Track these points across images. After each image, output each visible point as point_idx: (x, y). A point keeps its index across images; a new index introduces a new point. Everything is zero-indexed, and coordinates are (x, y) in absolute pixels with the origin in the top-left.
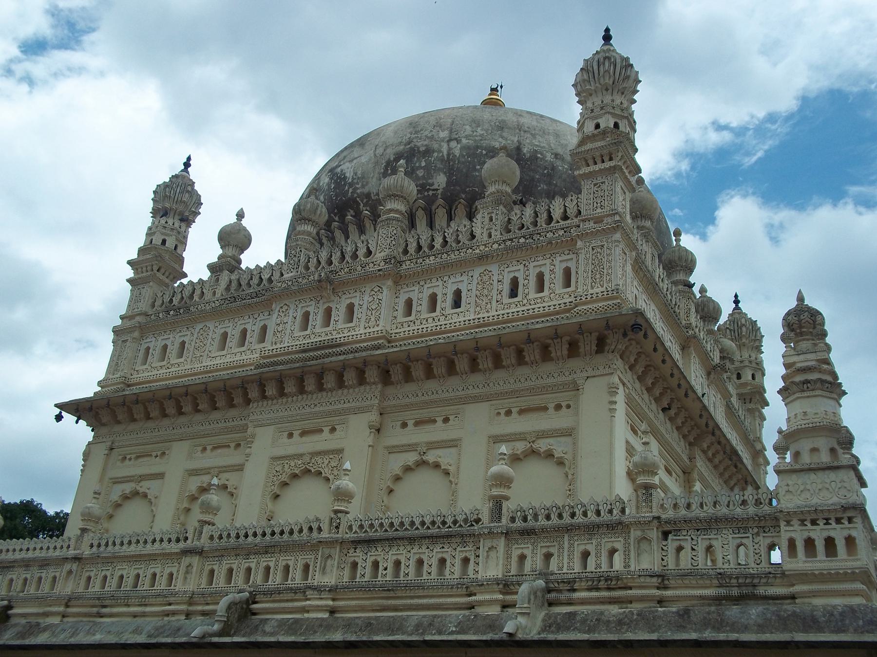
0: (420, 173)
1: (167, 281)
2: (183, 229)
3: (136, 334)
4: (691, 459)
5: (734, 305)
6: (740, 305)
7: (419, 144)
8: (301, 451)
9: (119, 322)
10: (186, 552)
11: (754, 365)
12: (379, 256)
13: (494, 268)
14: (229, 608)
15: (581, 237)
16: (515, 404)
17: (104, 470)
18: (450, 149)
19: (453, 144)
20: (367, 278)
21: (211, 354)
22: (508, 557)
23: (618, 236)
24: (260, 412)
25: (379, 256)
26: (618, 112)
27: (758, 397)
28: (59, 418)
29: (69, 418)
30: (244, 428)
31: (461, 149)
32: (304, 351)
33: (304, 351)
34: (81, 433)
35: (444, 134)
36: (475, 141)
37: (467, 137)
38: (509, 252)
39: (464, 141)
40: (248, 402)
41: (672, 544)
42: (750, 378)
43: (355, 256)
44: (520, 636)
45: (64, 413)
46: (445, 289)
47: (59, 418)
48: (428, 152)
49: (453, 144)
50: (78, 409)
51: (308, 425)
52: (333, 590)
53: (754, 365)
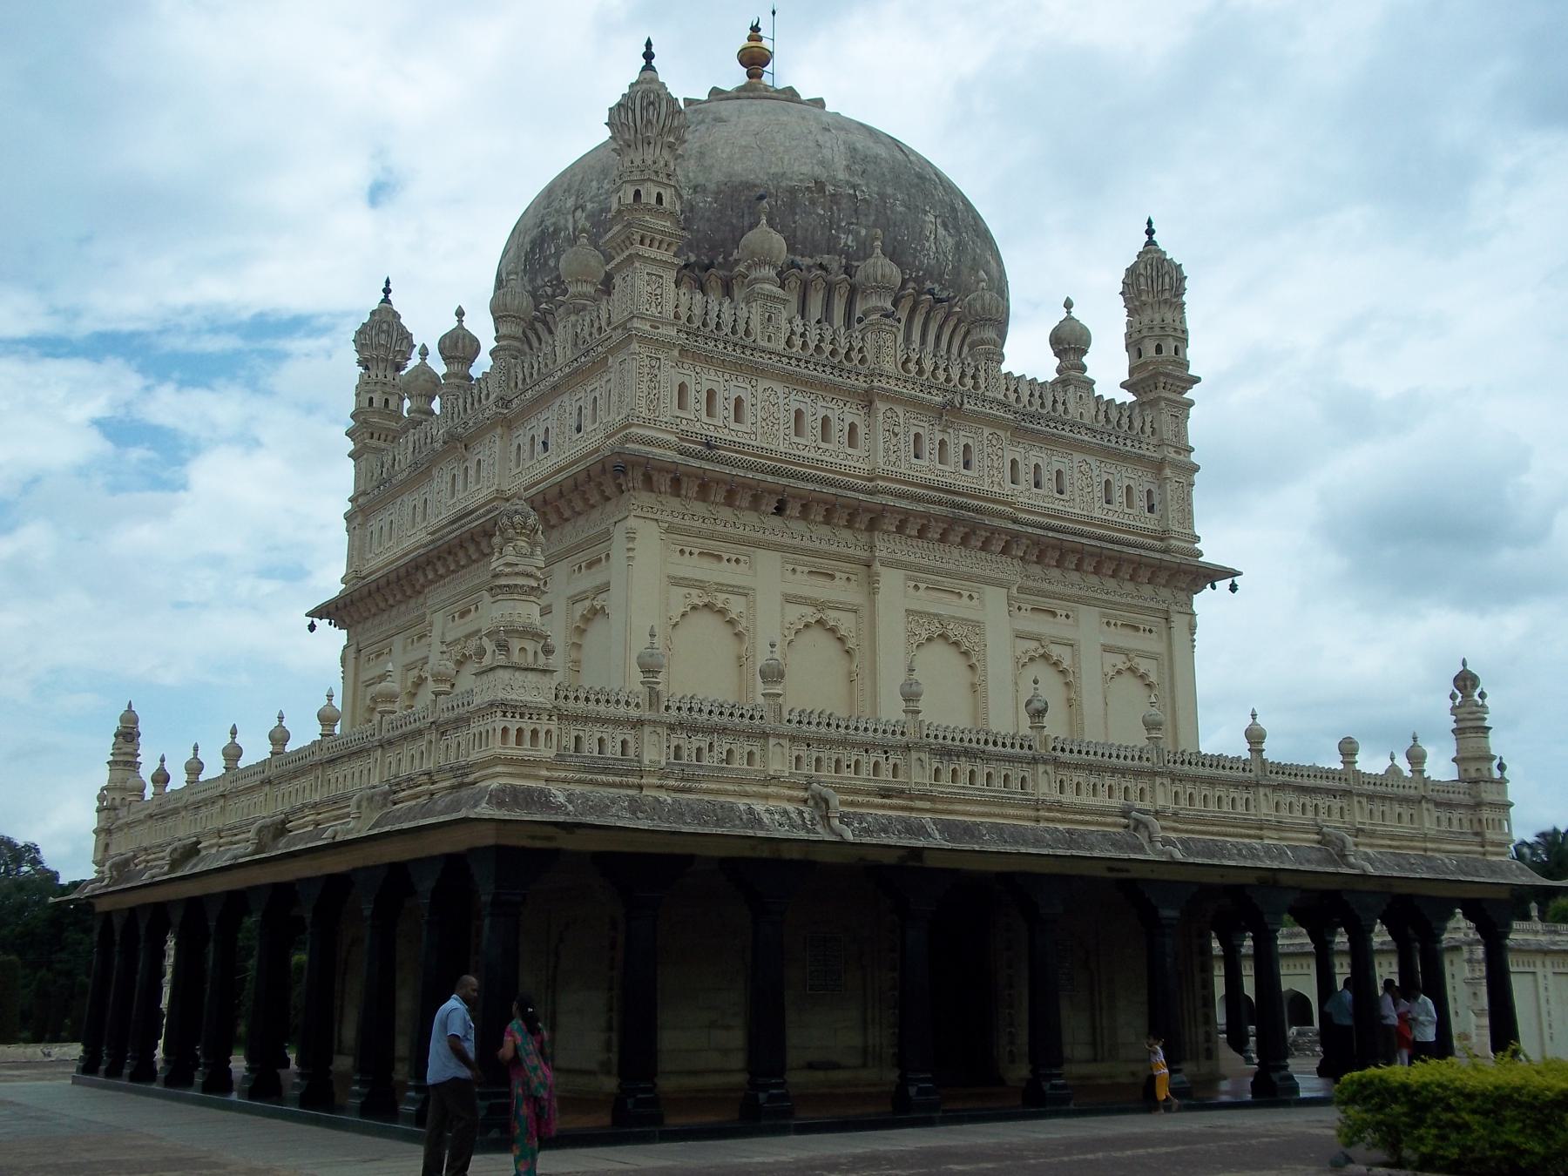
0: (552, 263)
1: (382, 445)
2: (390, 377)
3: (359, 520)
4: (872, 548)
5: (1146, 238)
6: (1155, 237)
7: (548, 223)
8: (460, 635)
9: (349, 506)
10: (262, 783)
11: (1157, 331)
12: (492, 397)
13: (566, 397)
14: (260, 831)
15: (611, 351)
16: (584, 557)
17: (356, 675)
18: (575, 222)
19: (579, 213)
20: (483, 430)
21: (409, 533)
22: (382, 766)
23: (635, 346)
24: (437, 596)
25: (492, 397)
26: (636, 176)
27: (1162, 379)
28: (312, 627)
29: (322, 624)
30: (422, 618)
31: (587, 218)
32: (453, 522)
33: (453, 522)
34: (333, 638)
35: (570, 203)
36: (600, 202)
37: (591, 201)
38: (578, 375)
39: (589, 206)
40: (423, 587)
41: (443, 744)
42: (1152, 352)
43: (480, 401)
44: (338, 839)
45: (316, 621)
46: (535, 427)
47: (312, 627)
48: (556, 231)
49: (579, 213)
50: (330, 611)
51: (460, 606)
52: (315, 805)
53: (1157, 331)
